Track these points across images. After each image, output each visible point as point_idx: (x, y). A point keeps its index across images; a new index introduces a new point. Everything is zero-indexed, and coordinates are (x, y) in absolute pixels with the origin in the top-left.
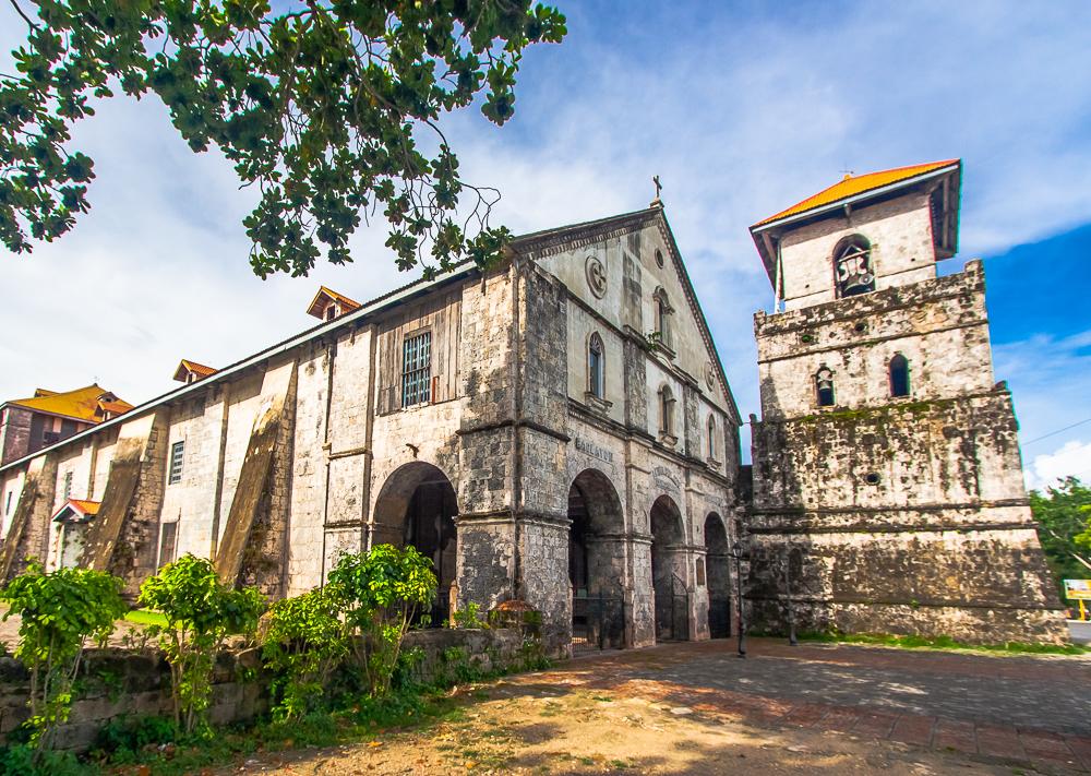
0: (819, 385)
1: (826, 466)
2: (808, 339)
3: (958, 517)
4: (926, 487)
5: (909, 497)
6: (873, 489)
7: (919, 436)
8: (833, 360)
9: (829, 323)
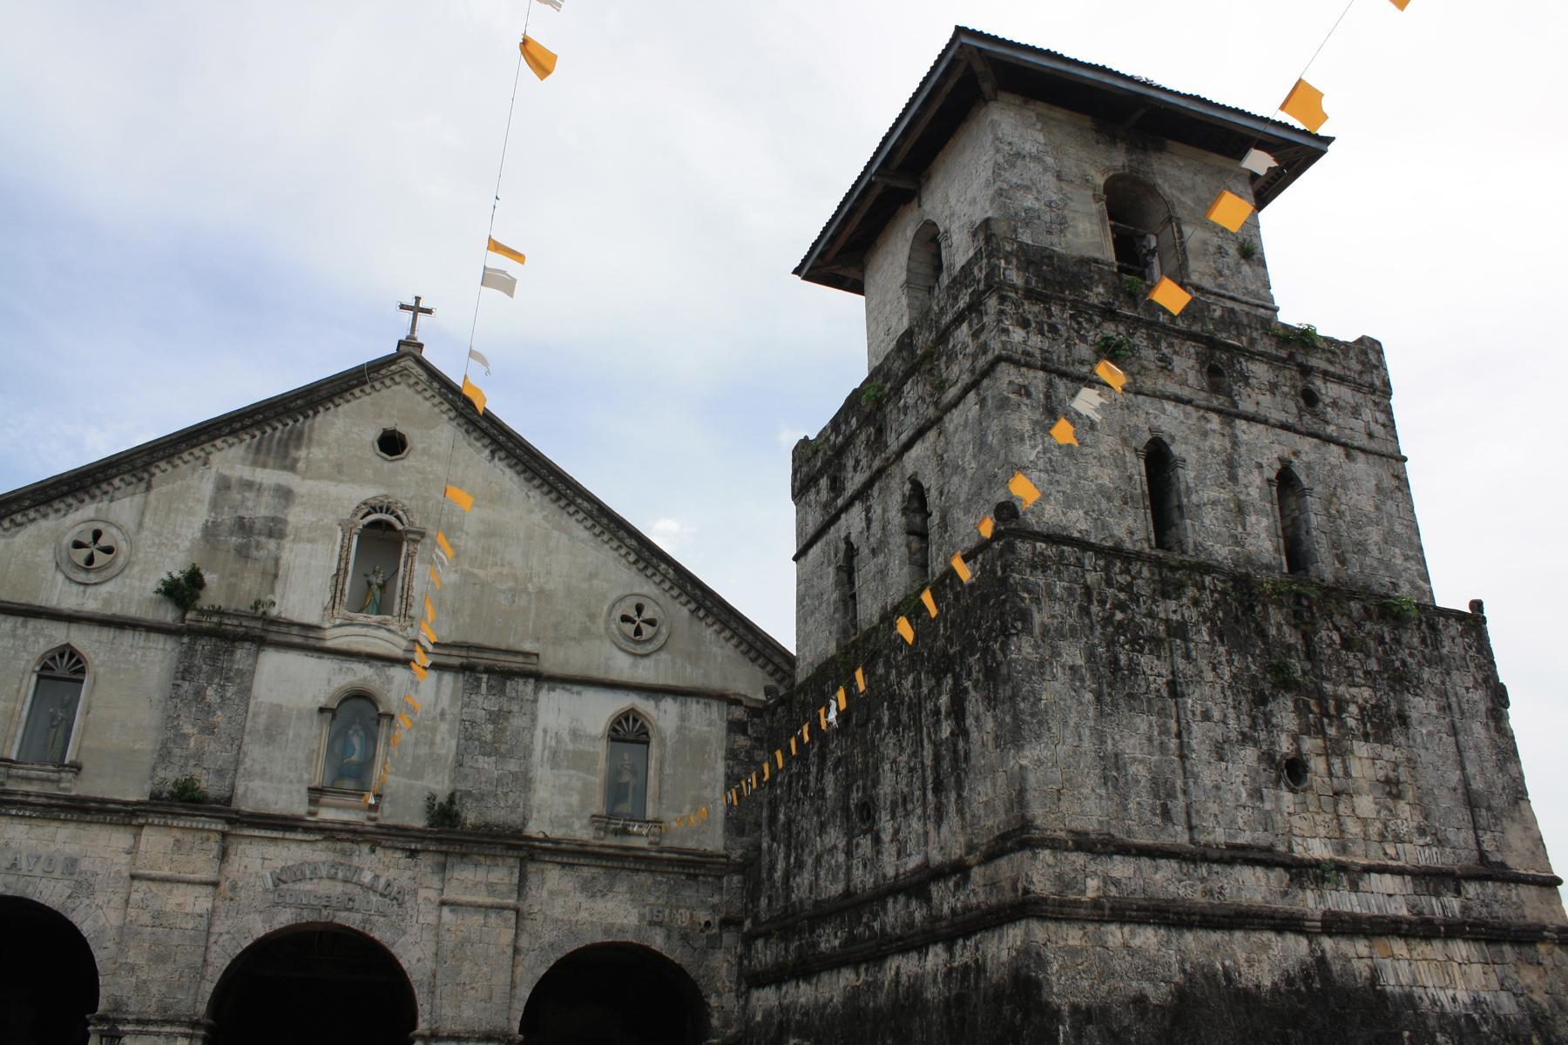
1: (823, 791)
2: (836, 486)
3: (945, 898)
8: (853, 521)
9: (850, 440)
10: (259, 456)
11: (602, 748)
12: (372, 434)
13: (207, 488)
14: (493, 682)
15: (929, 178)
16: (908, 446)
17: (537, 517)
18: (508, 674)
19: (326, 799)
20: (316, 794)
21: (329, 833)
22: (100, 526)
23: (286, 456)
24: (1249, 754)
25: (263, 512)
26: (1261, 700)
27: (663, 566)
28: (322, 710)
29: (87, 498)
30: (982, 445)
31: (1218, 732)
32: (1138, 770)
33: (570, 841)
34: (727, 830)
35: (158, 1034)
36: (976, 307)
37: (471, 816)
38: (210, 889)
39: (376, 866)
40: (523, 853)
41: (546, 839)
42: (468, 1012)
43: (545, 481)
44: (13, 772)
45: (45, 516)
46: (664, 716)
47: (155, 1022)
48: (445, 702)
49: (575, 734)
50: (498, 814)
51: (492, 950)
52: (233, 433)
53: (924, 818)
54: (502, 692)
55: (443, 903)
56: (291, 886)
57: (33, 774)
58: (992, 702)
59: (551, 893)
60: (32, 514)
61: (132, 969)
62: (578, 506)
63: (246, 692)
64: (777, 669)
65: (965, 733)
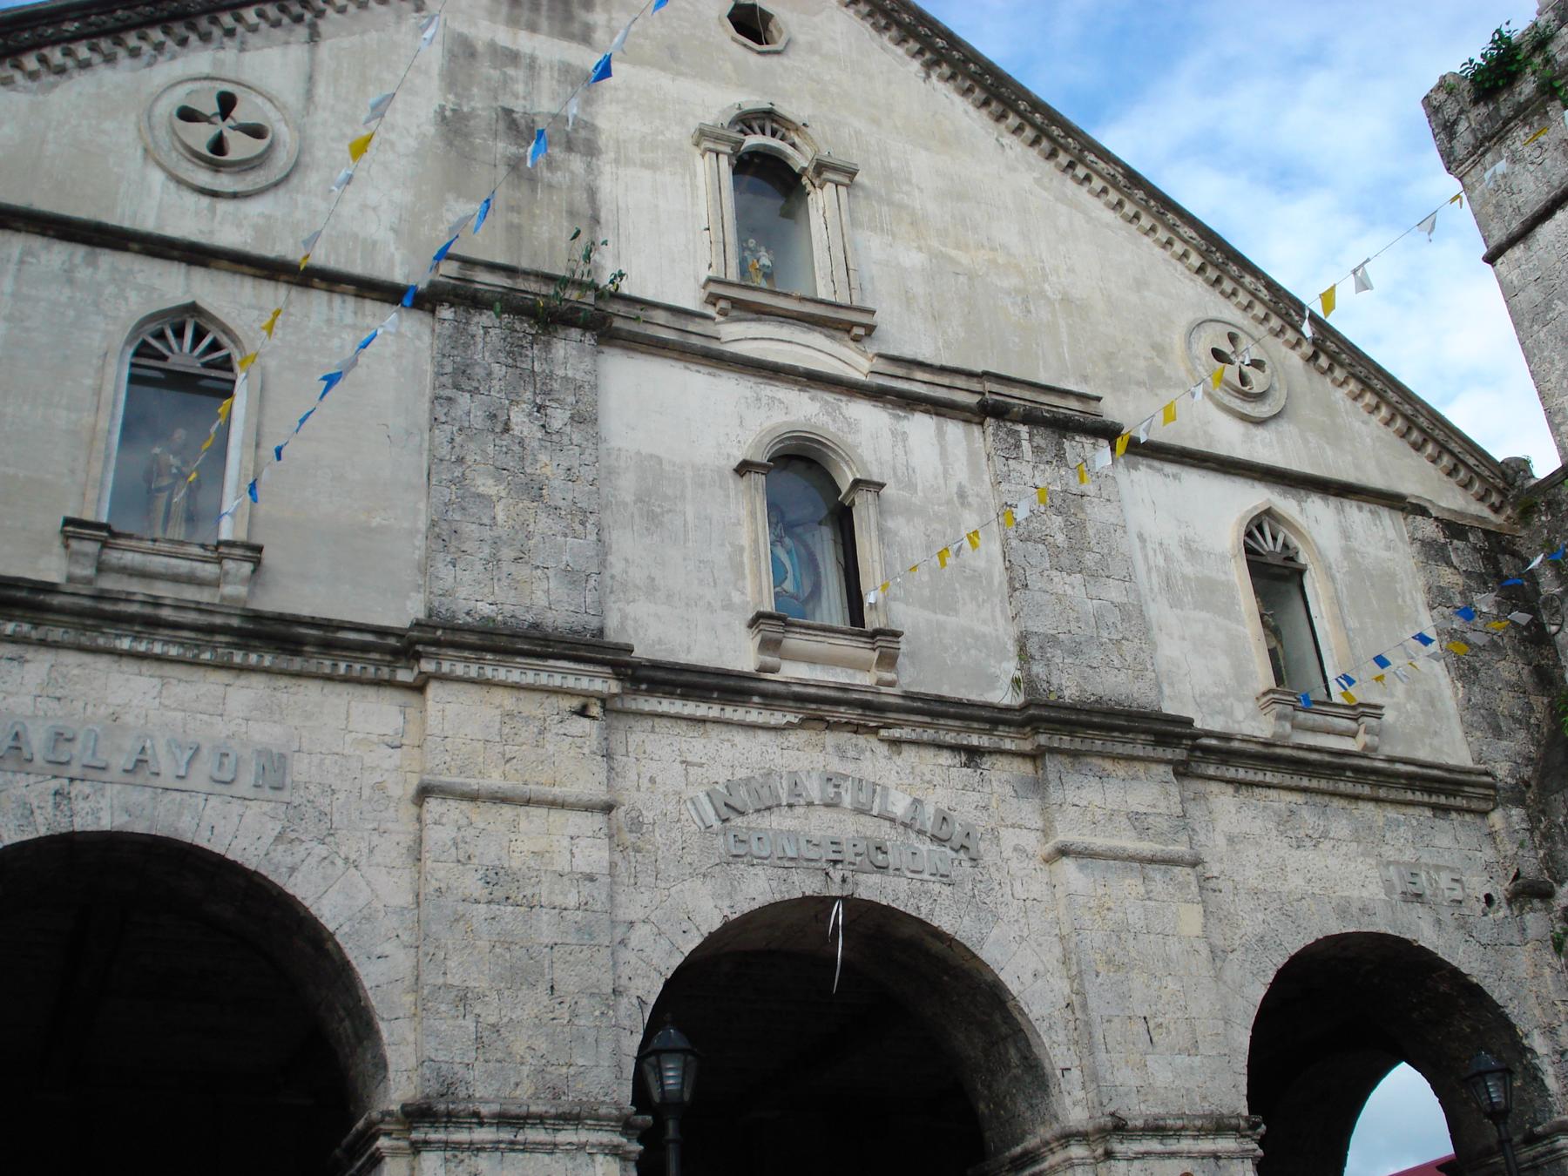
11: (1239, 576)
13: (434, 57)
14: (1038, 440)
18: (1064, 426)
19: (794, 641)
20: (773, 625)
23: (568, 17)
27: (1248, 279)
28: (744, 468)
29: (193, 38)
33: (1246, 740)
34: (1469, 729)
35: (552, 1148)
38: (598, 820)
39: (911, 780)
40: (1179, 754)
44: (113, 557)
45: (110, 59)
46: (1317, 525)
47: (540, 1120)
48: (961, 473)
50: (1114, 684)
51: (1174, 948)
54: (1061, 456)
55: (1063, 852)
56: (753, 820)
57: (158, 563)
59: (1231, 840)
60: (82, 51)
61: (464, 998)
63: (585, 418)
64: (1459, 462)
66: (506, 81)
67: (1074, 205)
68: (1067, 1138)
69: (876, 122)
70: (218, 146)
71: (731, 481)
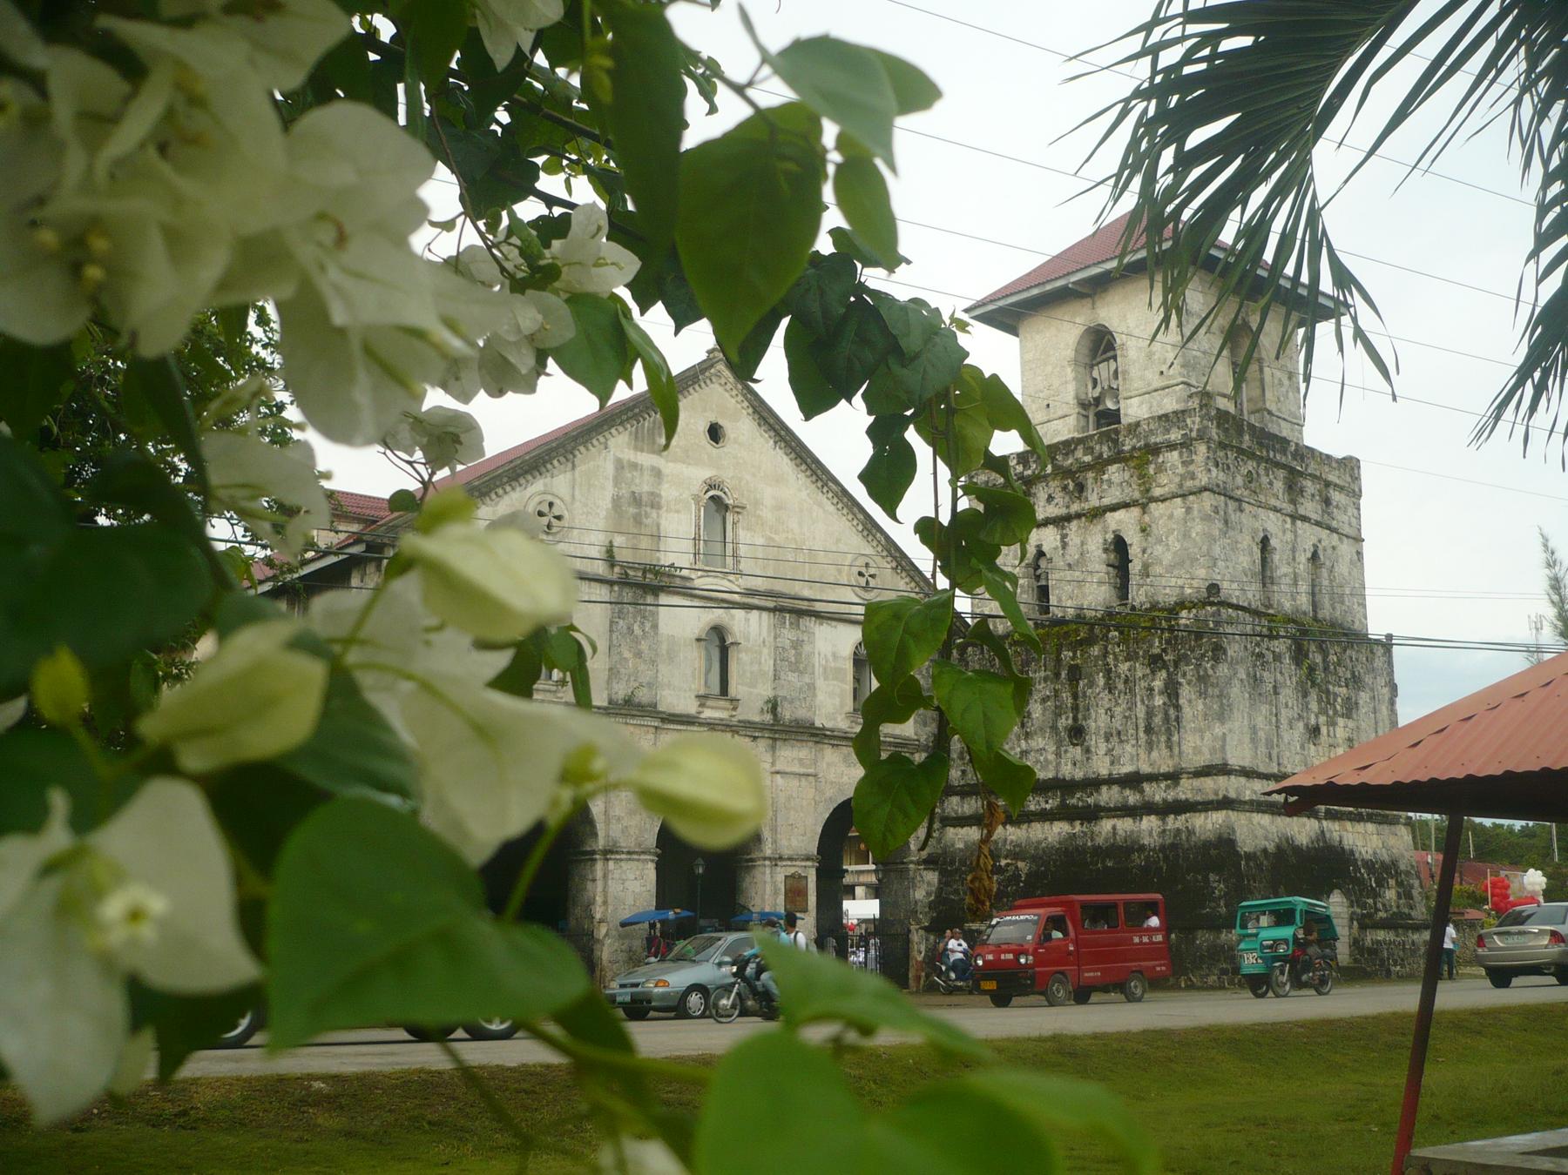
0: (1038, 578)
1: (1029, 713)
3: (1157, 793)
4: (1128, 748)
5: (1112, 763)
6: (1077, 752)
7: (1124, 667)
10: (638, 442)
11: (849, 666)
12: (703, 427)
13: (610, 469)
15: (1105, 290)
16: (1114, 508)
17: (804, 494)
18: (800, 613)
19: (709, 703)
21: (712, 725)
22: (550, 498)
24: (1301, 725)
25: (646, 488)
26: (1305, 695)
28: (698, 640)
30: (1186, 535)
31: (1291, 713)
32: (1261, 734)
36: (1186, 445)
37: (787, 713)
41: (824, 729)
42: (795, 843)
43: (809, 467)
49: (834, 655)
50: (802, 713)
52: (621, 423)
53: (1137, 745)
58: (1203, 694)
61: (619, 819)
62: (830, 489)
63: (655, 627)
65: (1178, 707)
66: (633, 478)
67: (820, 505)
68: (765, 859)
69: (754, 475)
70: (549, 526)
71: (695, 644)
